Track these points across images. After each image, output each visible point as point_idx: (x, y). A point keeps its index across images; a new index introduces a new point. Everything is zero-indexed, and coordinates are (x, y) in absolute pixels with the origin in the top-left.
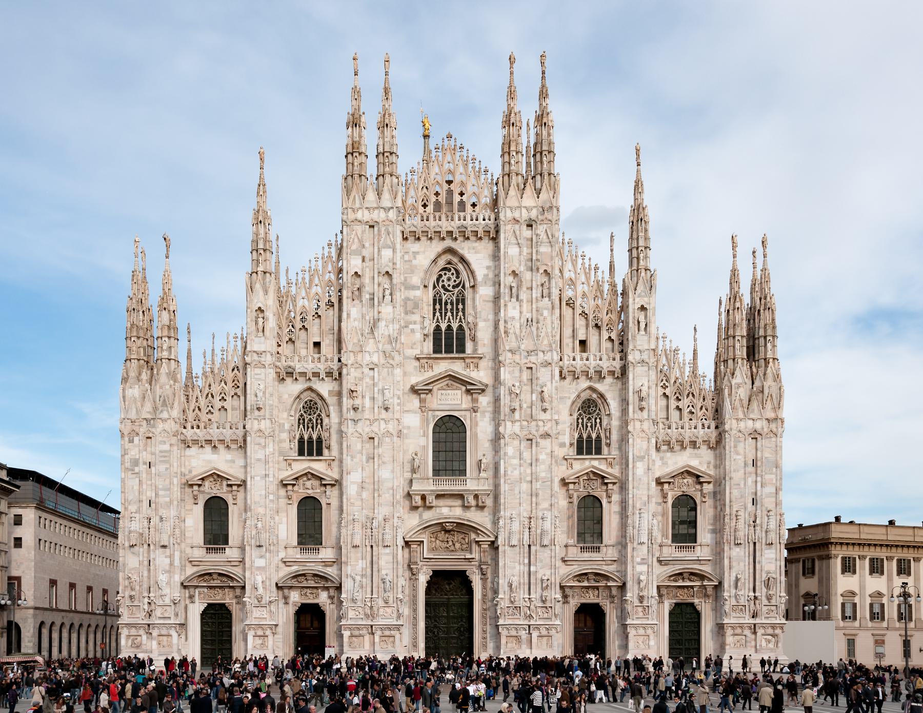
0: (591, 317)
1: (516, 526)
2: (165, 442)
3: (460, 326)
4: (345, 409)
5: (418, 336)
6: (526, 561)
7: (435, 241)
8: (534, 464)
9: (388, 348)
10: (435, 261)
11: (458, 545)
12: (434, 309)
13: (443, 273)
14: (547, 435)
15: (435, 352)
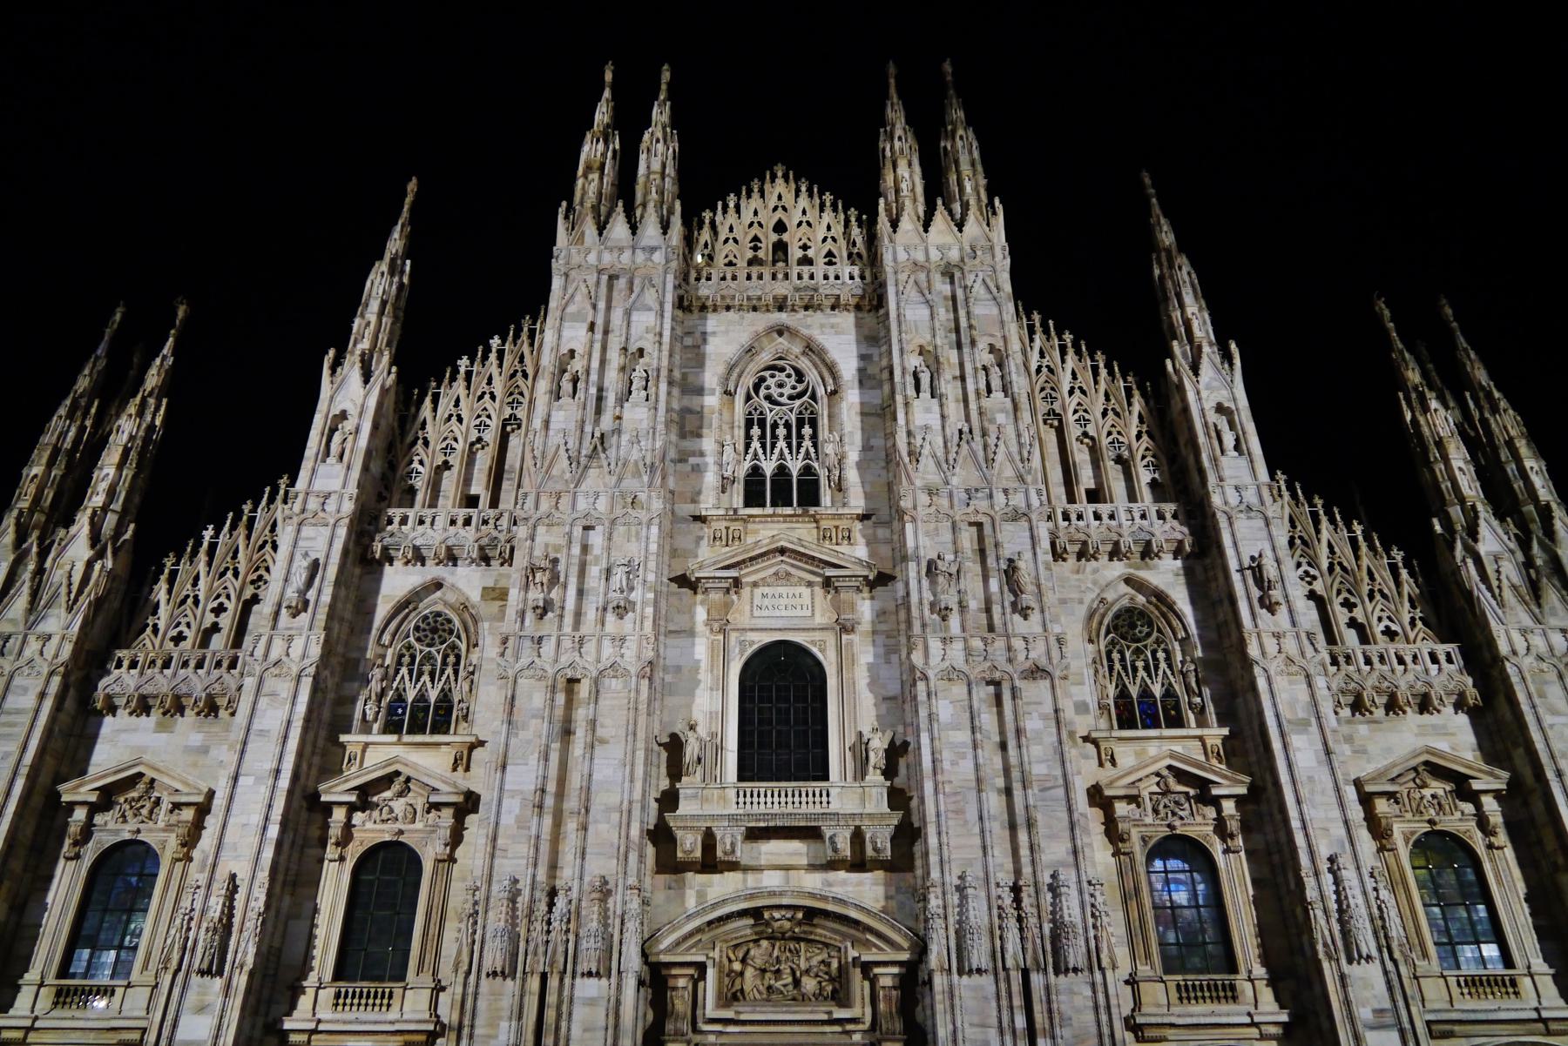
0: (1105, 441)
1: (978, 913)
2: (25, 690)
3: (807, 470)
4: (511, 613)
5: (711, 479)
6: (1020, 1022)
7: (752, 314)
8: (1011, 744)
9: (630, 484)
10: (750, 351)
11: (809, 984)
12: (748, 437)
13: (767, 374)
14: (1036, 672)
15: (747, 504)
